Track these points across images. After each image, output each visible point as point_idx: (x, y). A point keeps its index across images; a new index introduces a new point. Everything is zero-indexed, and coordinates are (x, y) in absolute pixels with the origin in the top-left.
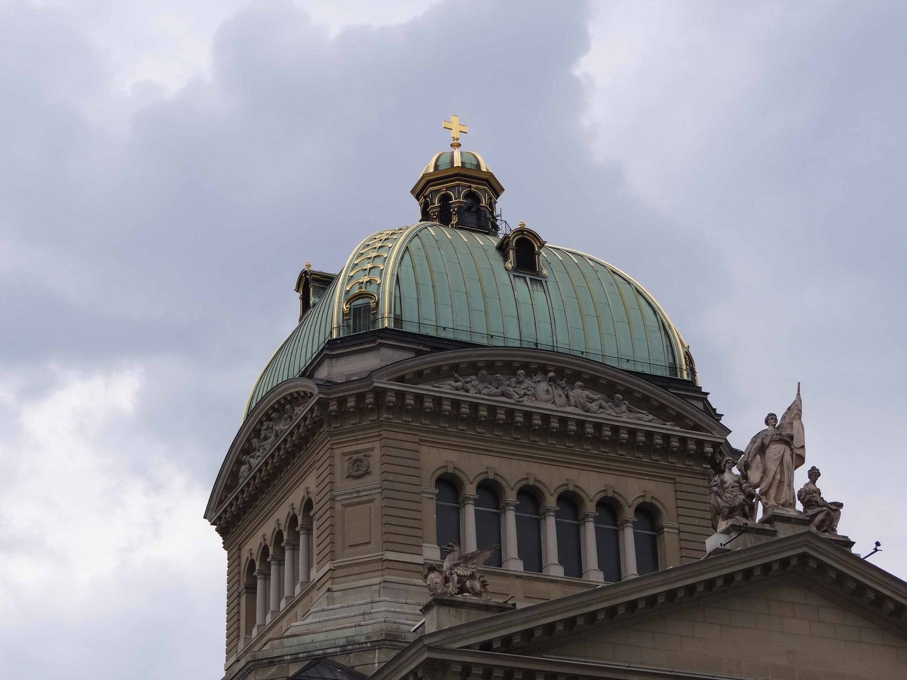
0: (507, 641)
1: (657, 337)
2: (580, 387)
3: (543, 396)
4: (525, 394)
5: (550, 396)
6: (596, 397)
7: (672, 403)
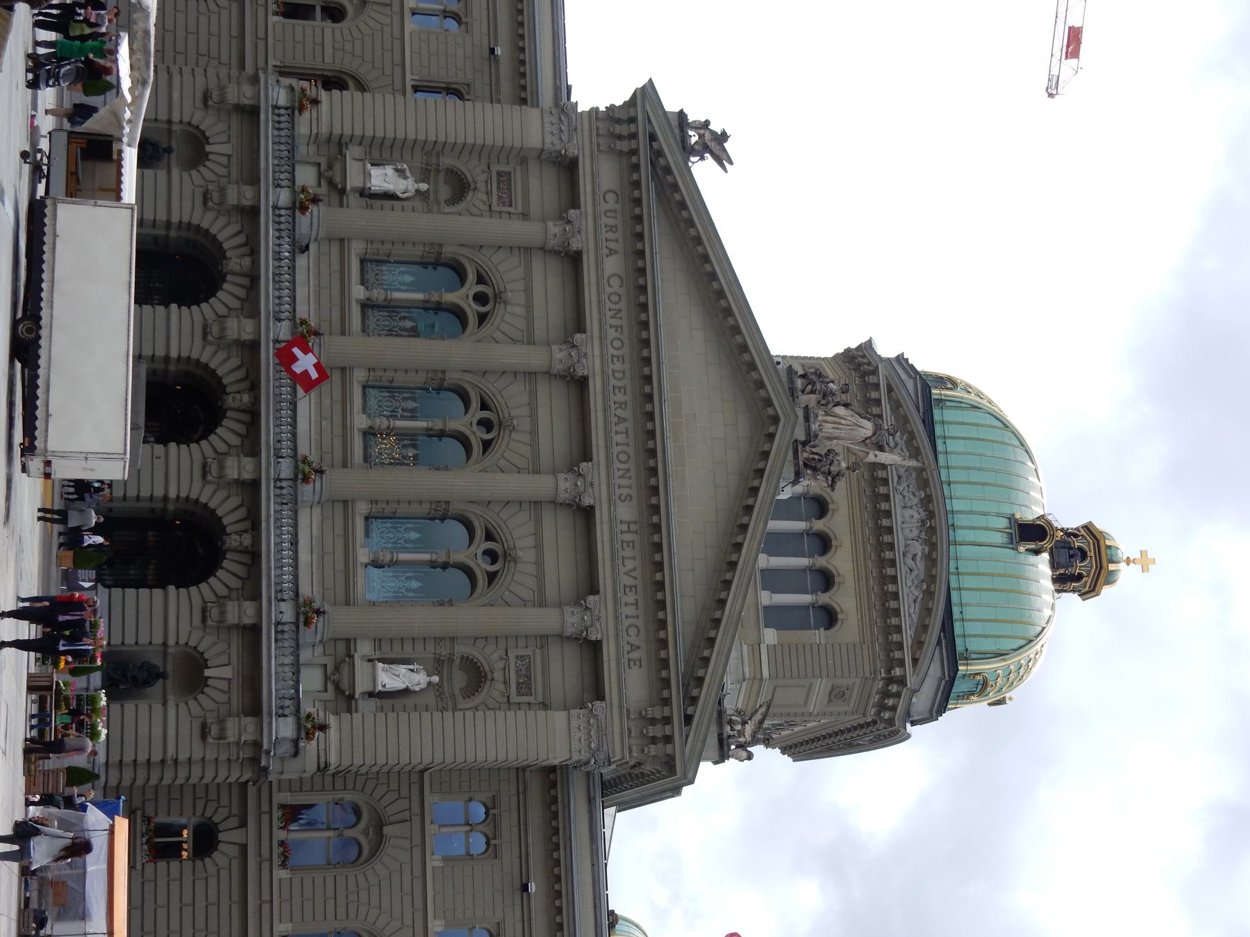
0: (659, 153)
1: (989, 645)
2: (924, 549)
3: (908, 512)
4: (904, 497)
5: (908, 520)
6: (918, 562)
7: (931, 636)
